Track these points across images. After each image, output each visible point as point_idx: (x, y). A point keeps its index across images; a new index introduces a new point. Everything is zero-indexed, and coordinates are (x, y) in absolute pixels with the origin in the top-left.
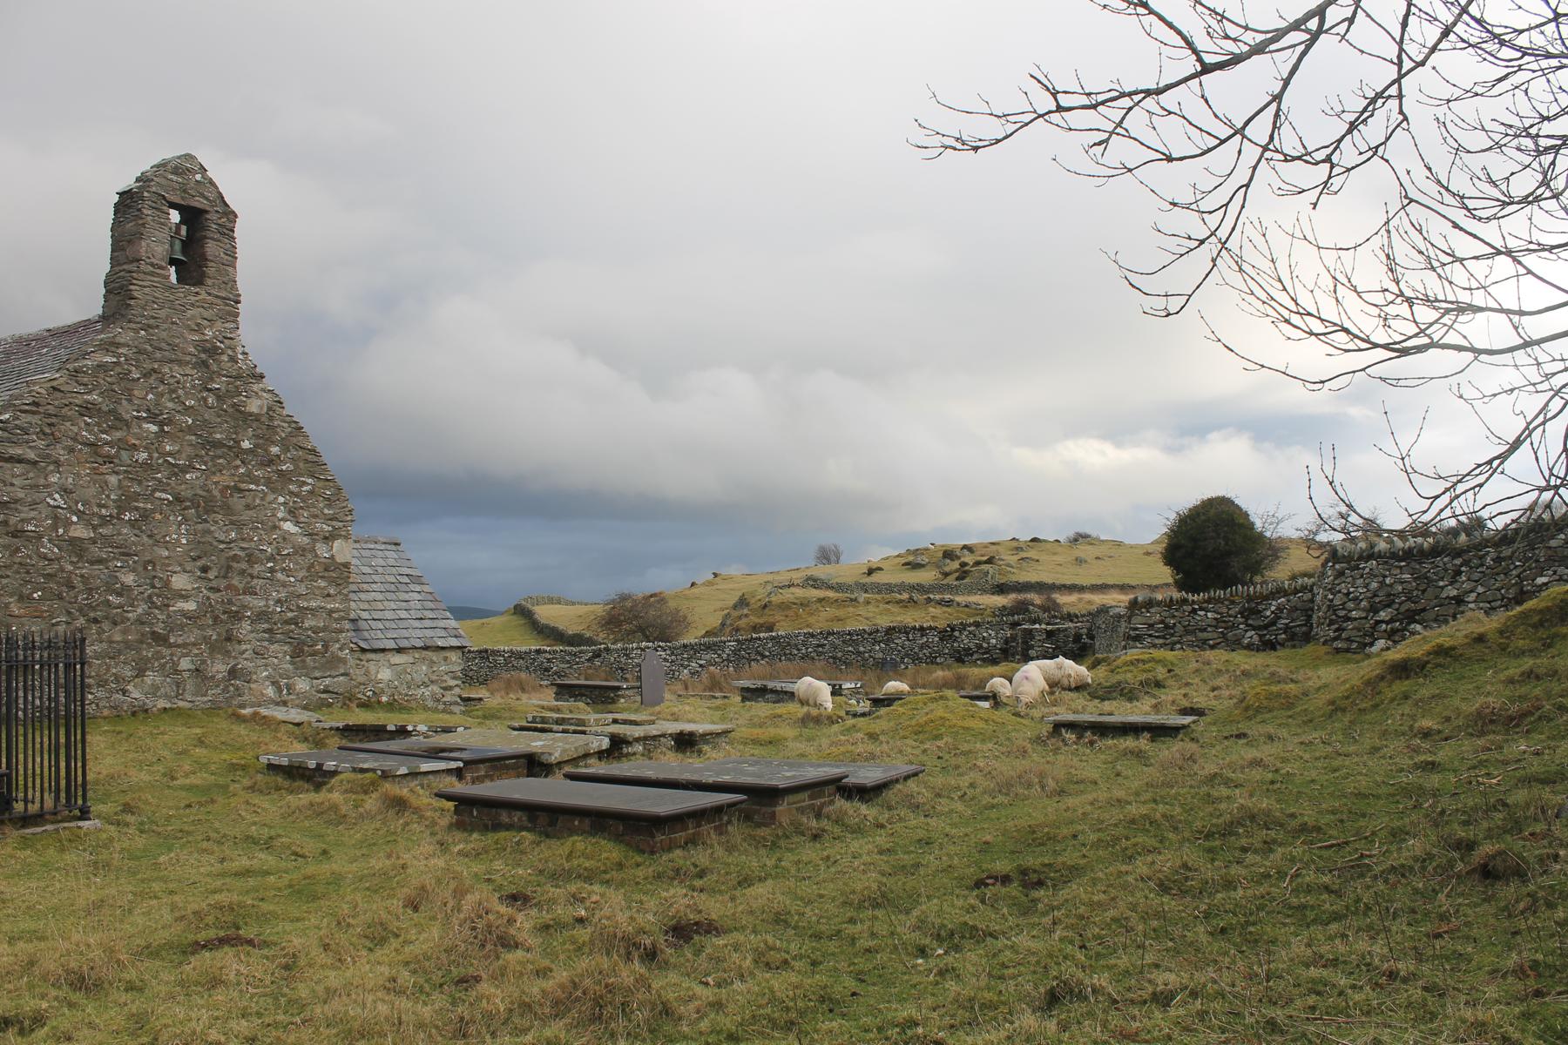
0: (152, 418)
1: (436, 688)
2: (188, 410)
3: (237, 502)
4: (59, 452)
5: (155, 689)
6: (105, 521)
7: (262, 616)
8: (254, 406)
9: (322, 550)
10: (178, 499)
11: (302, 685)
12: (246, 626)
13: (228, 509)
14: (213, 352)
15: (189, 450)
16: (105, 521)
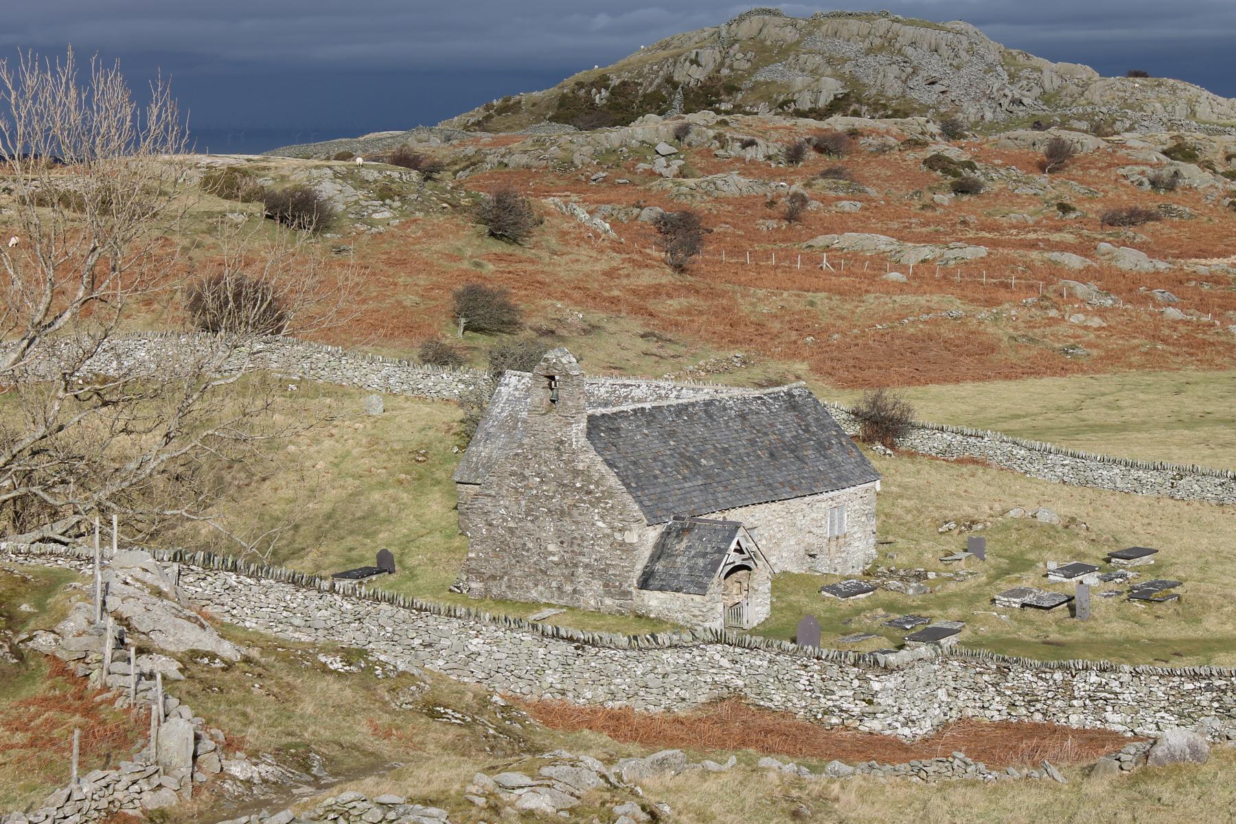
0: (538, 475)
1: (686, 615)
2: (552, 471)
3: (575, 512)
4: (504, 492)
5: (541, 594)
6: (521, 520)
7: (586, 566)
8: (580, 467)
9: (618, 536)
10: (550, 511)
11: (608, 601)
12: (581, 570)
13: (570, 515)
14: (562, 442)
15: (553, 489)
16: (521, 520)
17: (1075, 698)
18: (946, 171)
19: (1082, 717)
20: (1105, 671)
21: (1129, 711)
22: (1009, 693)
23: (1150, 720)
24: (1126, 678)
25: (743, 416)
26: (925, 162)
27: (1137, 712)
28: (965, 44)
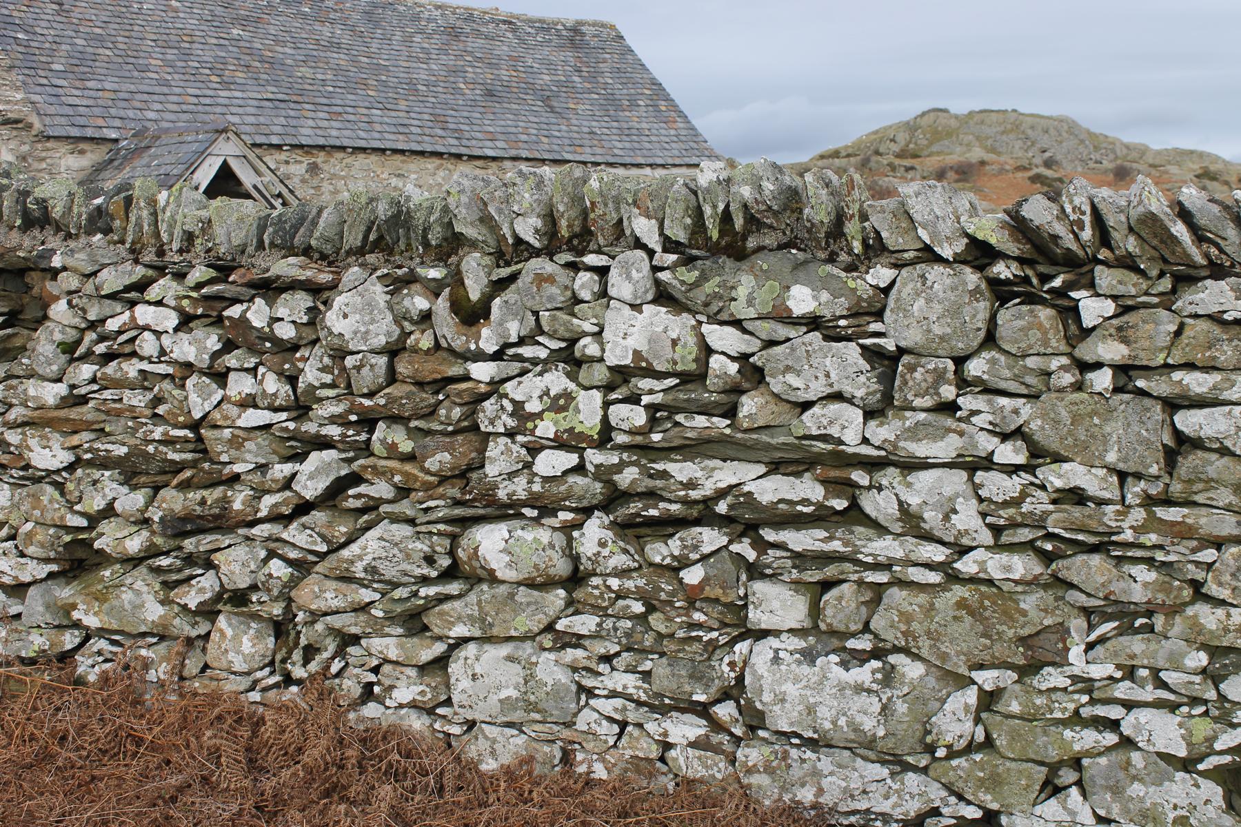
17: (506, 511)
18: (1043, 184)
19: (551, 669)
20: (734, 247)
21: (961, 640)
22: (48, 454)
23: (1164, 732)
24: (931, 307)
25: (454, 33)
26: (1029, 178)
27: (1036, 655)
28: (1066, 127)
